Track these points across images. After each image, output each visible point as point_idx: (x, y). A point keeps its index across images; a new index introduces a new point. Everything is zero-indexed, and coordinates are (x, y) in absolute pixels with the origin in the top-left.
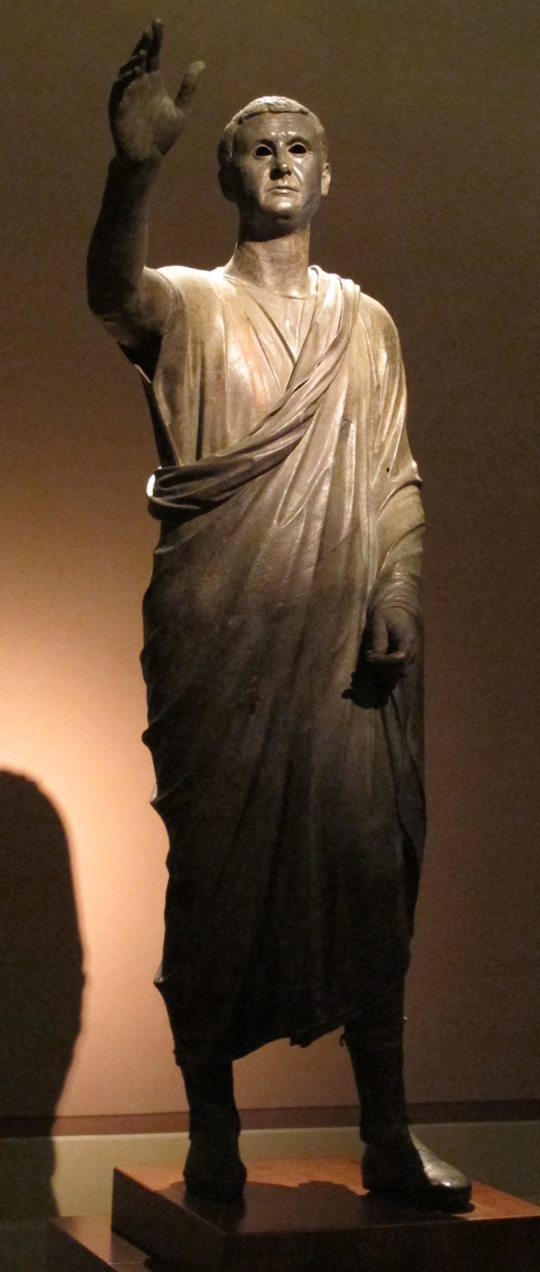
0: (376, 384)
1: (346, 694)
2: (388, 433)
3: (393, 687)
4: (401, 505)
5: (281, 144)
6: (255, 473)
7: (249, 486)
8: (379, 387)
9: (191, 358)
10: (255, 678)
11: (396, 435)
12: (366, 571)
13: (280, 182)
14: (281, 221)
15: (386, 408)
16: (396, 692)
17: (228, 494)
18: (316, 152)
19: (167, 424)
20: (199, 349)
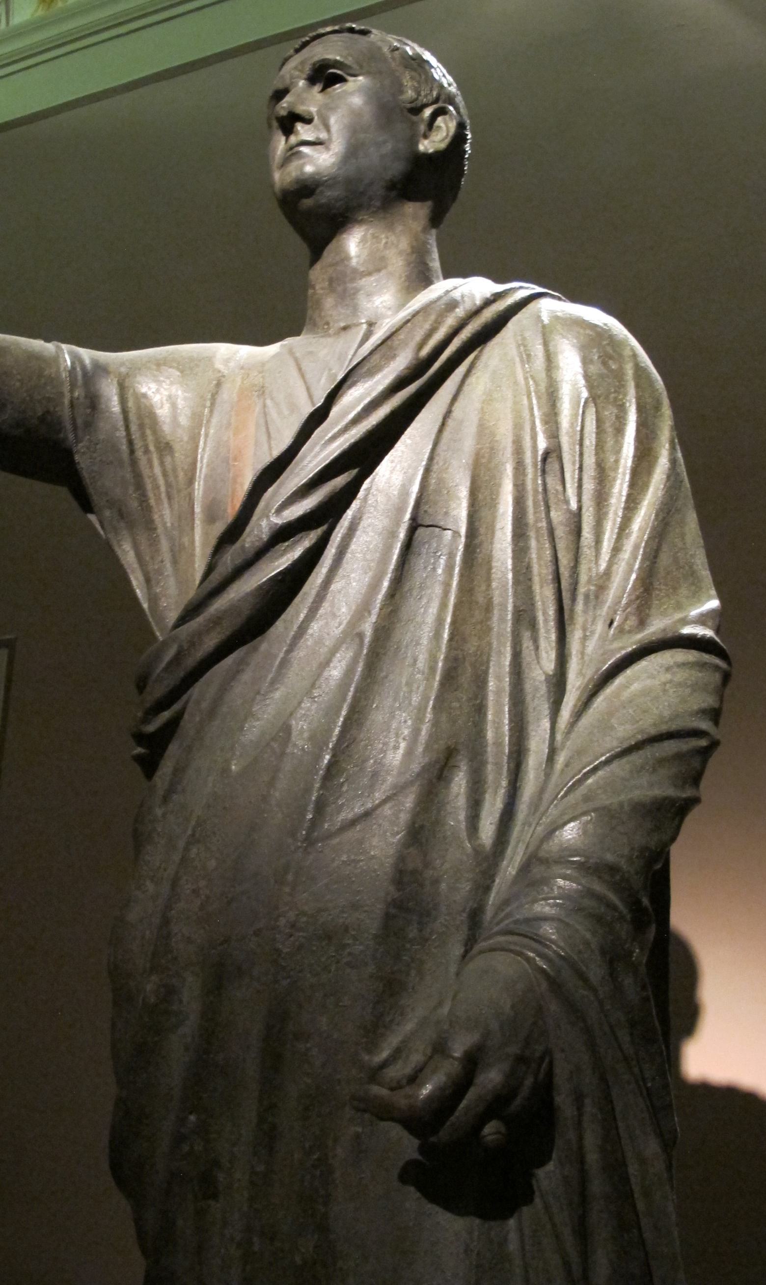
0: (542, 444)
1: (411, 1174)
2: (616, 549)
3: (542, 1163)
4: (626, 695)
5: (302, 83)
6: (190, 662)
7: (195, 691)
8: (553, 454)
9: (161, 481)
10: (192, 1118)
11: (636, 547)
12: (489, 862)
13: (293, 139)
14: (307, 203)
15: (601, 498)
16: (548, 1176)
17: (166, 715)
18: (367, 74)
19: (145, 606)
20: (168, 460)
